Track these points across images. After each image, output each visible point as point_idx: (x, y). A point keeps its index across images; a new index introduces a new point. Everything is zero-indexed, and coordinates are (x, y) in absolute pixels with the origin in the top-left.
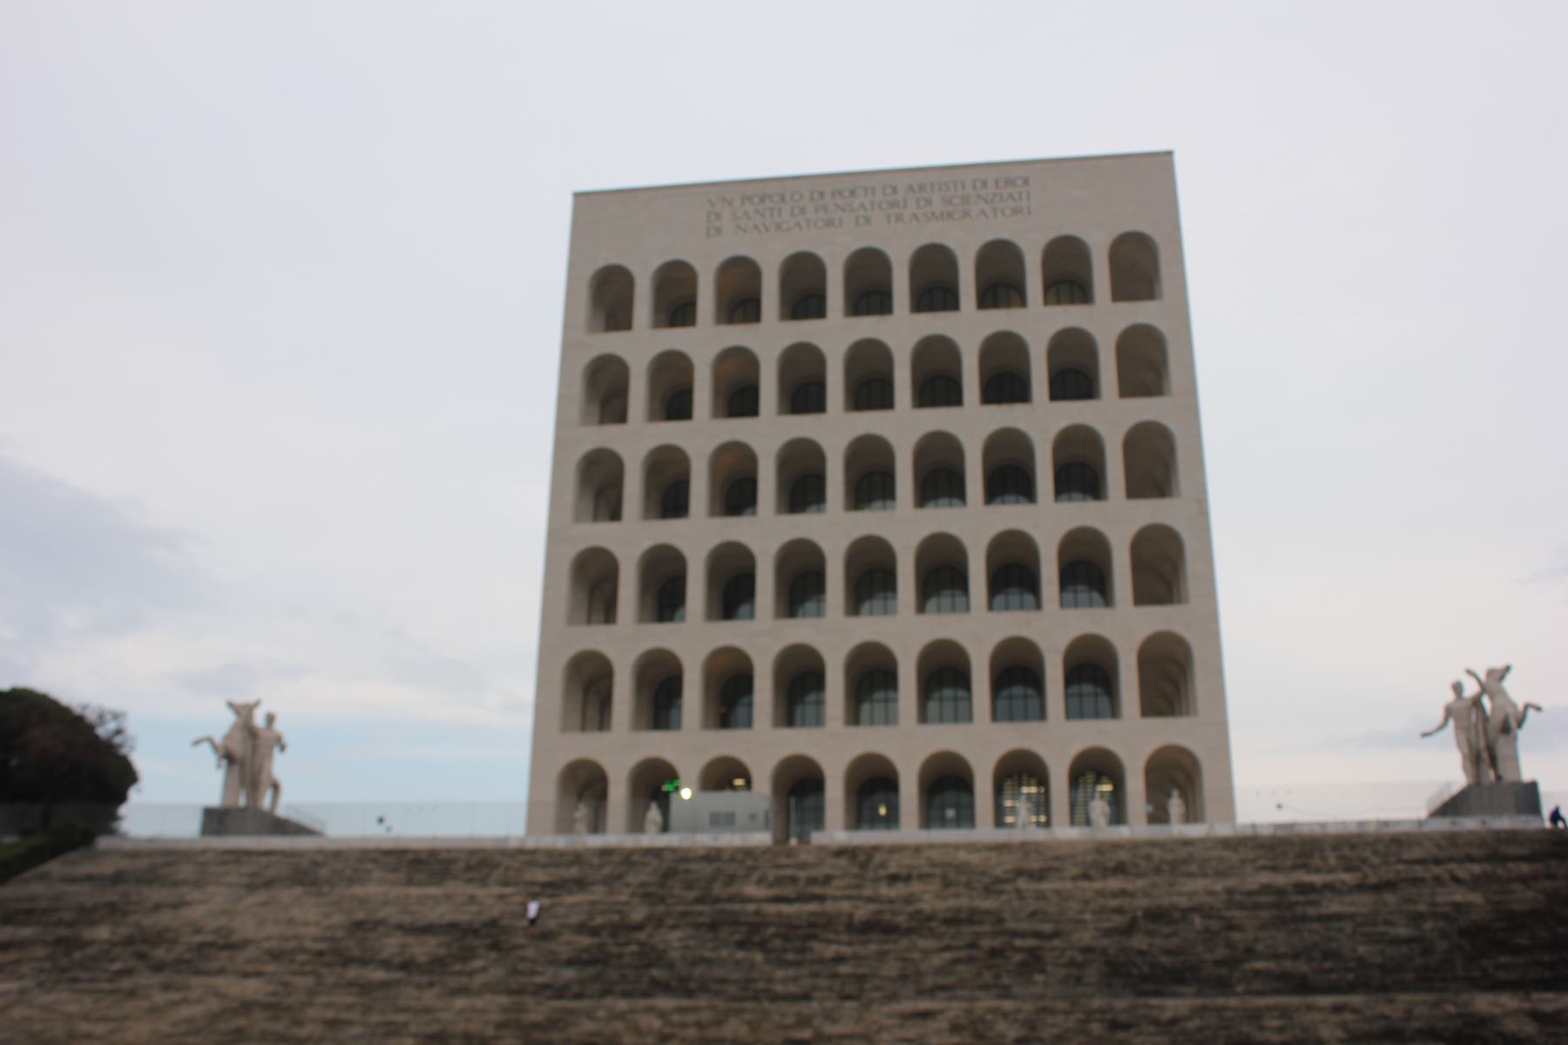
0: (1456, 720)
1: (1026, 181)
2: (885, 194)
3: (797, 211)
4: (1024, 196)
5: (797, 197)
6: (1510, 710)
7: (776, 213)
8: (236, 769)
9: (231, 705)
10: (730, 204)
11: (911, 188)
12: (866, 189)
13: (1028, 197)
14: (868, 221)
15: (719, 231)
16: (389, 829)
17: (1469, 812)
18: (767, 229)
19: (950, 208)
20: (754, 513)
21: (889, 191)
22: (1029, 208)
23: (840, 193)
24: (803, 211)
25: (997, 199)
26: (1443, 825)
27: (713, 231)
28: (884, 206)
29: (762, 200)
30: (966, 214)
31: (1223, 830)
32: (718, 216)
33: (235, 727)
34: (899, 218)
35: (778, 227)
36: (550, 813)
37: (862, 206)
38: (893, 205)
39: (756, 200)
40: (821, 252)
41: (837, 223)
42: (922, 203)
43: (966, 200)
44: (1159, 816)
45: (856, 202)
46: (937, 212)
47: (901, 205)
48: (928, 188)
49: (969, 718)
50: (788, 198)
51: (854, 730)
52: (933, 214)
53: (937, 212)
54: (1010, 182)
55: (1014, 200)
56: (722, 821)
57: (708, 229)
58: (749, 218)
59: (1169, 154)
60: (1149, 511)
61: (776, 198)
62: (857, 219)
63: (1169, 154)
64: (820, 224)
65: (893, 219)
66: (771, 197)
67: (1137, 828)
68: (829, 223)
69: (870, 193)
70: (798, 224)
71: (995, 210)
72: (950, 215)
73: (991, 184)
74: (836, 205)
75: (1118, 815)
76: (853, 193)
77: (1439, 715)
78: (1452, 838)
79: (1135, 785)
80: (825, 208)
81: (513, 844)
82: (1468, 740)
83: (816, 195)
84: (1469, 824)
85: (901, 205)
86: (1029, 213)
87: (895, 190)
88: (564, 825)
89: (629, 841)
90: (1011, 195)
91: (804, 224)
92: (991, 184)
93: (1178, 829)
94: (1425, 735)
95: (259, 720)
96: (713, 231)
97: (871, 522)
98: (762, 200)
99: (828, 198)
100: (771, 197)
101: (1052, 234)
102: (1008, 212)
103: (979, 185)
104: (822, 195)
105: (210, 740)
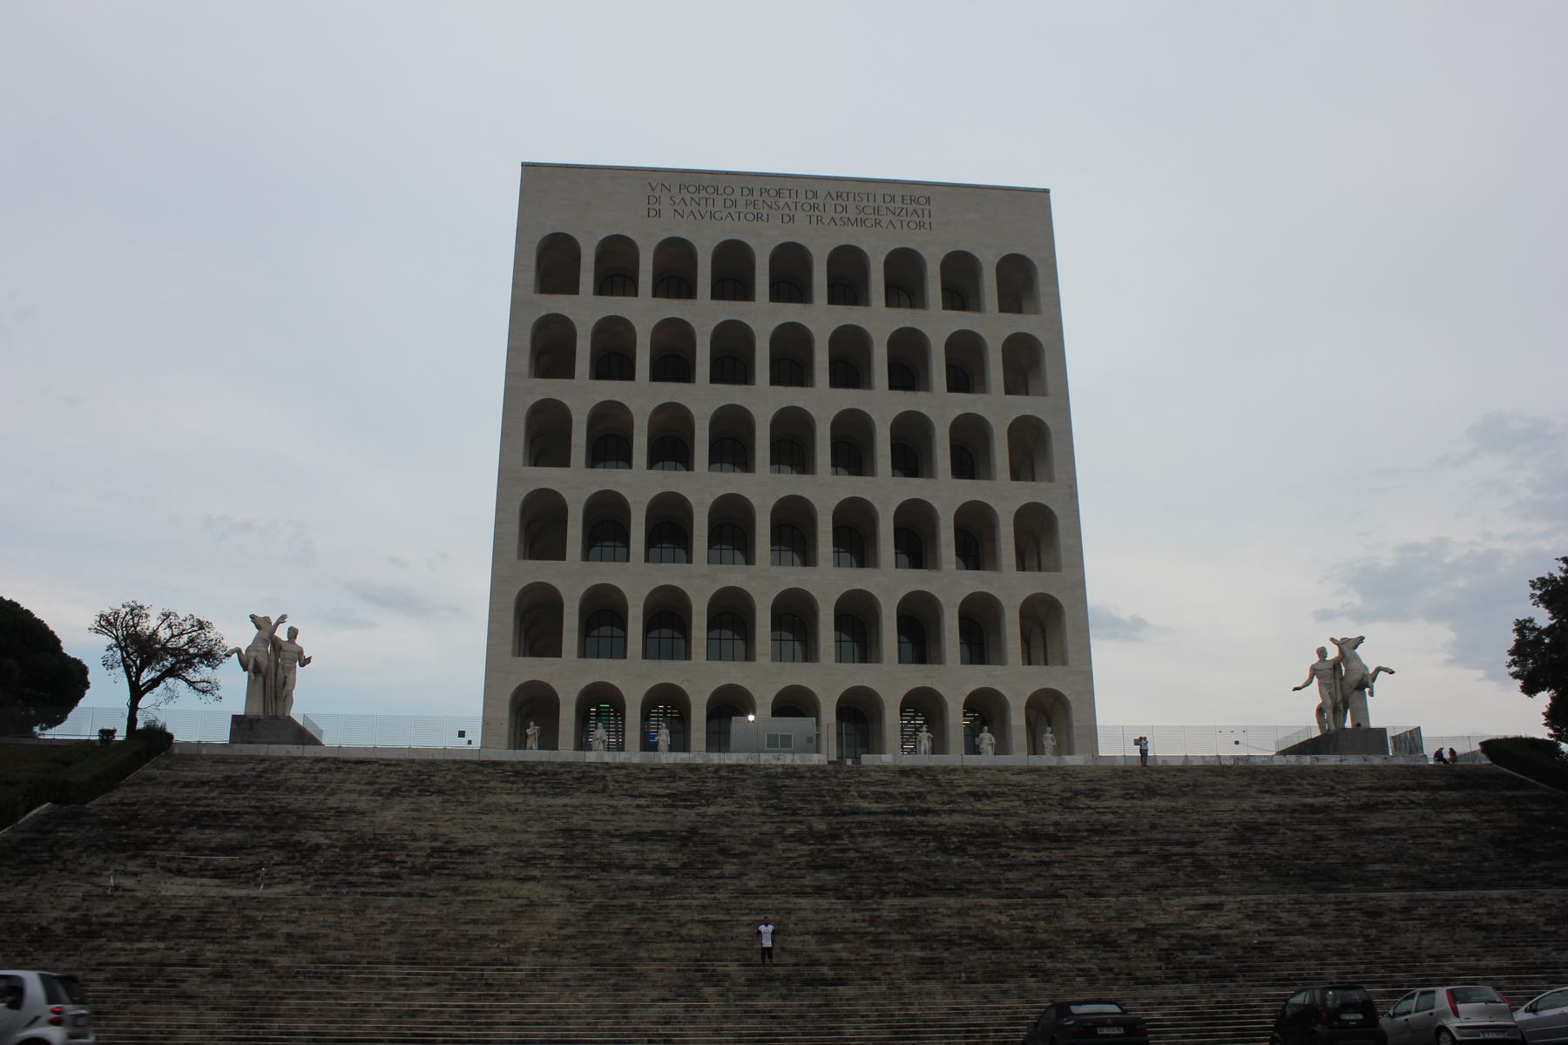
0: (1318, 678)
1: (928, 200)
3: (729, 203)
4: (926, 212)
5: (729, 191)
6: (1366, 672)
7: (710, 202)
8: (260, 679)
9: (253, 617)
10: (670, 191)
12: (790, 190)
14: (792, 219)
15: (658, 213)
16: (470, 742)
17: (1335, 751)
19: (864, 217)
20: (953, 478)
21: (810, 195)
24: (734, 203)
25: (904, 210)
26: (1292, 760)
27: (653, 213)
28: (807, 207)
29: (698, 190)
30: (877, 223)
31: (1075, 760)
32: (658, 200)
33: (257, 639)
35: (712, 215)
36: (505, 729)
38: (814, 207)
39: (692, 189)
40: (751, 242)
41: (765, 217)
42: (839, 209)
43: (877, 210)
44: (1035, 747)
45: (782, 202)
47: (821, 208)
49: (878, 660)
50: (721, 191)
51: (778, 664)
54: (914, 200)
56: (781, 743)
58: (686, 205)
59: (1047, 191)
60: (1027, 492)
61: (711, 190)
64: (750, 217)
65: (814, 219)
67: (1019, 756)
68: (758, 217)
69: (793, 195)
72: (863, 222)
75: (939, 746)
76: (778, 193)
77: (1306, 675)
78: (1302, 772)
79: (1017, 719)
81: (475, 758)
82: (1330, 693)
83: (746, 192)
84: (1331, 760)
85: (821, 208)
87: (815, 195)
88: (519, 741)
89: (609, 757)
91: (735, 216)
92: (898, 199)
93: (1048, 760)
94: (1295, 689)
95: (282, 633)
96: (653, 213)
97: (610, 479)
98: (698, 190)
99: (757, 194)
101: (950, 250)
102: (913, 225)
103: (888, 199)
104: (751, 191)
105: (238, 651)
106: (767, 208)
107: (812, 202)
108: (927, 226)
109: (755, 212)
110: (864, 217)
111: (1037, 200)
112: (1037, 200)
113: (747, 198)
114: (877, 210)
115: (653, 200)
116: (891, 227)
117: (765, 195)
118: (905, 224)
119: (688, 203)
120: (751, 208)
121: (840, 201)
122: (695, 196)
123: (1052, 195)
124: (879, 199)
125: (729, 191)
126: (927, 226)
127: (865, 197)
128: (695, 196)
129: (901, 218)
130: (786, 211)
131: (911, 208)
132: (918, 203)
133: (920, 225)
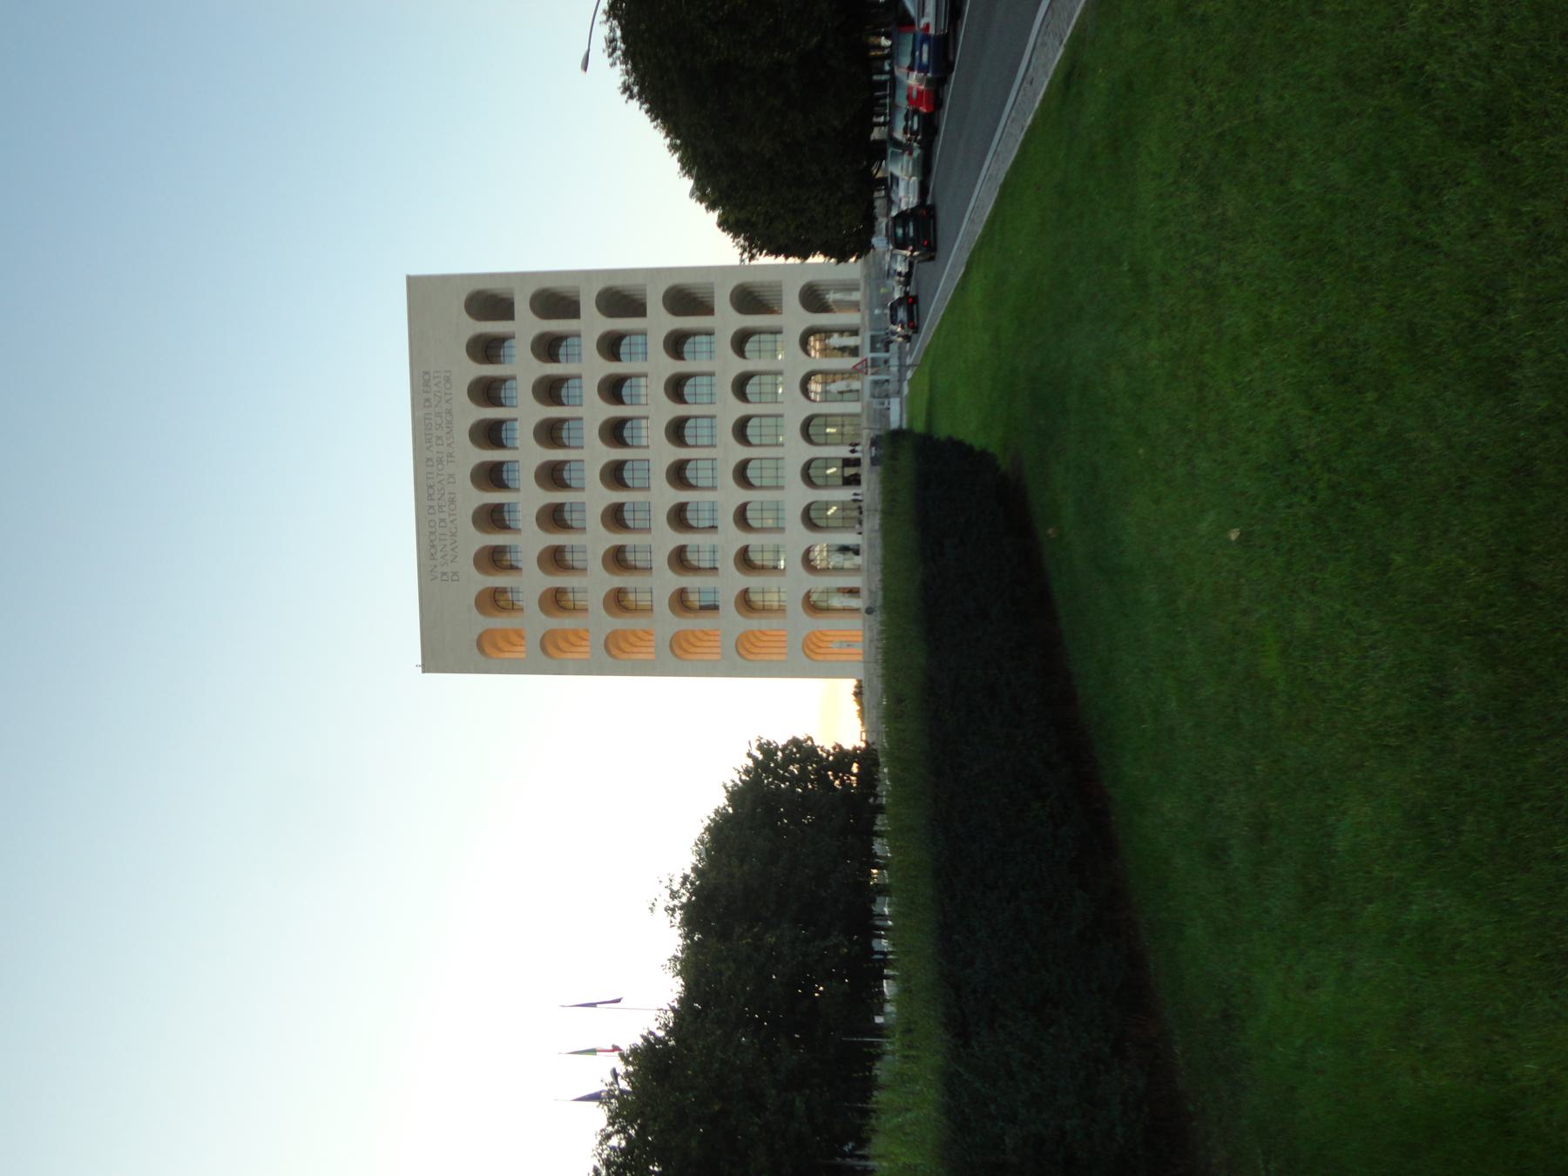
1: (426, 373)
2: (432, 466)
7: (442, 537)
10: (436, 566)
11: (427, 448)
13: (439, 372)
14: (451, 476)
15: (455, 573)
18: (456, 541)
21: (430, 463)
22: (446, 372)
23: (430, 495)
24: (443, 520)
28: (440, 467)
29: (433, 546)
32: (444, 574)
34: (451, 455)
37: (440, 482)
39: (433, 551)
43: (438, 415)
46: (446, 430)
47: (440, 455)
48: (429, 437)
52: (448, 433)
53: (446, 430)
54: (426, 383)
55: (440, 382)
57: (453, 580)
59: (414, 284)
61: (433, 537)
62: (449, 483)
63: (414, 284)
64: (452, 507)
65: (449, 459)
66: (432, 541)
68: (452, 501)
70: (452, 522)
71: (446, 394)
74: (439, 499)
76: (431, 487)
80: (440, 507)
86: (449, 372)
87: (428, 460)
90: (436, 385)
98: (433, 546)
99: (434, 503)
100: (432, 541)
102: (448, 386)
103: (427, 404)
104: (431, 507)
107: (436, 463)
108: (448, 374)
109: (448, 503)
110: (445, 421)
111: (420, 289)
112: (420, 289)
113: (437, 510)
114: (438, 415)
115: (445, 578)
116: (451, 402)
117: (433, 497)
118: (449, 392)
119: (443, 554)
120: (444, 509)
121: (434, 440)
122: (439, 548)
125: (432, 524)
126: (448, 374)
127: (427, 422)
128: (439, 548)
129: (443, 394)
130: (443, 482)
131: (435, 388)
132: (429, 380)
133: (448, 380)
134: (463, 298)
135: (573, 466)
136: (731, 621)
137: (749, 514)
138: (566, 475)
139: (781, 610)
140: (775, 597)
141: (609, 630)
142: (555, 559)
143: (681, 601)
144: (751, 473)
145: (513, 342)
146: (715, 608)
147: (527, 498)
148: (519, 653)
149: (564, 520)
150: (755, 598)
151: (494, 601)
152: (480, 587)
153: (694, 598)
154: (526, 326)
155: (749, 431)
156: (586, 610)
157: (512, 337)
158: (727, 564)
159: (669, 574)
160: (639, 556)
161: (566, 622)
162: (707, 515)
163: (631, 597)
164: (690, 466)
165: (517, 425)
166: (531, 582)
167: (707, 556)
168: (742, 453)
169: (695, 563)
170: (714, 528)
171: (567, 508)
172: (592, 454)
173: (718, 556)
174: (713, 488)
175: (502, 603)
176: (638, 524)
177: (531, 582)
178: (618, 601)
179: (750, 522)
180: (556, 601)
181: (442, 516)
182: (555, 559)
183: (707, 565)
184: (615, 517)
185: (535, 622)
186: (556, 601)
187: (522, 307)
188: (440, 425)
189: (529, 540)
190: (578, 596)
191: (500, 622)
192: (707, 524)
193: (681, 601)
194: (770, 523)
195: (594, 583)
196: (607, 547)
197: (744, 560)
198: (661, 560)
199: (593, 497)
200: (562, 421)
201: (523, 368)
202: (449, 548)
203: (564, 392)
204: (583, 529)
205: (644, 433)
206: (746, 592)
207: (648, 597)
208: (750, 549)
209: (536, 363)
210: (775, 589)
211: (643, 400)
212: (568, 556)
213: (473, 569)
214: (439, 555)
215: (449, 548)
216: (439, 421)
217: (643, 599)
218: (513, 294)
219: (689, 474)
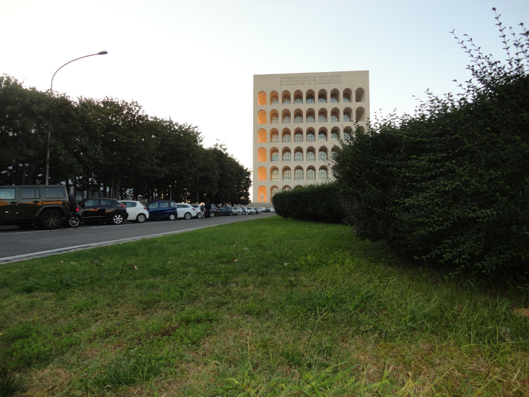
1: (341, 76)
14: (311, 84)
15: (282, 85)
24: (298, 81)
32: (282, 81)
34: (317, 83)
43: (328, 80)
54: (338, 76)
59: (367, 72)
63: (367, 72)
68: (303, 84)
73: (334, 77)
76: (308, 78)
80: (302, 81)
92: (334, 77)
98: (290, 78)
106: (305, 82)
111: (365, 74)
112: (365, 74)
114: (328, 80)
123: (369, 72)
124: (330, 76)
133: (339, 83)
134: (362, 87)
135: (313, 119)
136: (269, 165)
137: (299, 170)
138: (310, 117)
139: (271, 179)
140: (275, 178)
141: (266, 130)
142: (286, 114)
143: (274, 150)
144: (311, 170)
145: (348, 102)
146: (272, 161)
147: (304, 106)
148: (259, 103)
149: (297, 116)
150: (275, 172)
151: (274, 96)
152: (278, 92)
153: (275, 154)
154: (354, 105)
155: (323, 170)
156: (271, 123)
157: (350, 101)
158: (285, 164)
159: (283, 147)
160: (287, 138)
161: (268, 117)
162: (299, 158)
163: (275, 136)
164: (313, 154)
165: (325, 103)
166: (280, 107)
167: (287, 158)
168: (317, 168)
169: (285, 154)
170: (295, 160)
171: (301, 118)
172: (317, 125)
173: (287, 161)
174: (307, 160)
175: (273, 98)
176: (296, 138)
177: (280, 107)
178: (274, 132)
179: (297, 170)
180: (274, 114)
181: (299, 81)
182: (286, 114)
183: (284, 158)
184: (299, 131)
185: (268, 108)
186: (274, 114)
187: (359, 104)
188: (325, 80)
189: (292, 106)
190: (275, 121)
191: (268, 98)
192: (296, 158)
193: (274, 150)
194: (296, 176)
195: (280, 125)
196: (291, 129)
197: (287, 169)
198: (287, 145)
199: (305, 126)
200: (326, 117)
201: (342, 105)
202: (290, 83)
203: (334, 117)
204: (294, 122)
205: (322, 140)
206: (277, 169)
207: (275, 141)
208: (289, 171)
209: (343, 108)
210: (278, 178)
211: (332, 140)
212: (287, 118)
213: (284, 90)
214: (288, 80)
215: (290, 83)
216: (327, 80)
217: (274, 139)
218: (365, 101)
219: (311, 153)
